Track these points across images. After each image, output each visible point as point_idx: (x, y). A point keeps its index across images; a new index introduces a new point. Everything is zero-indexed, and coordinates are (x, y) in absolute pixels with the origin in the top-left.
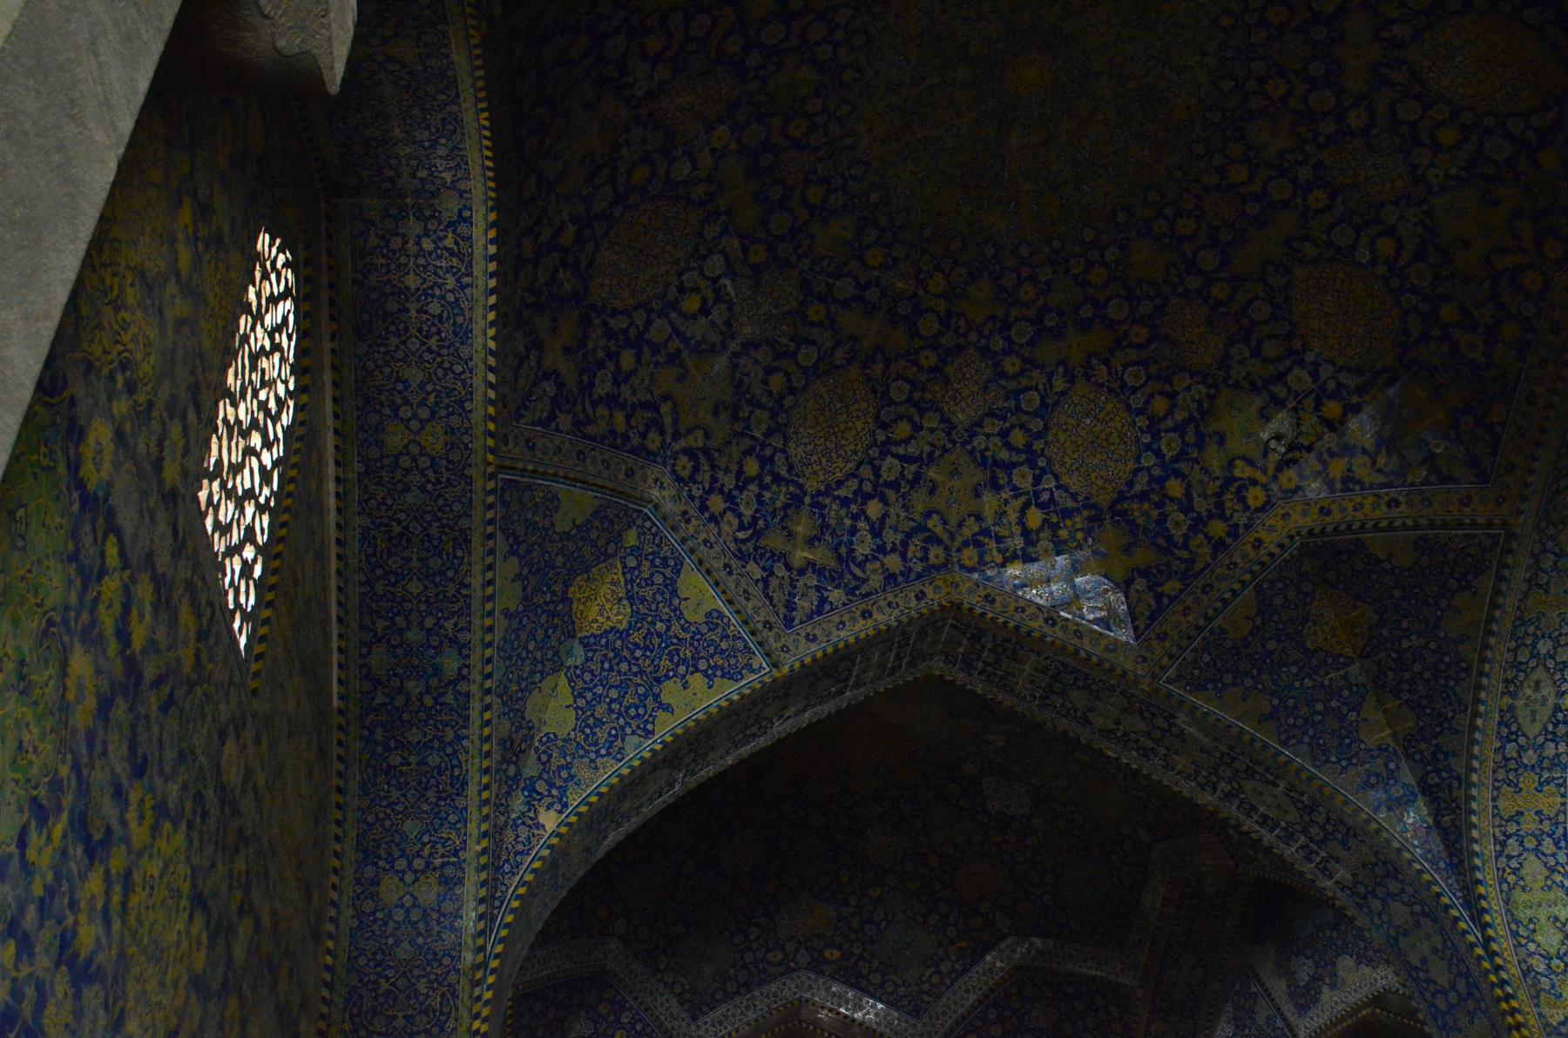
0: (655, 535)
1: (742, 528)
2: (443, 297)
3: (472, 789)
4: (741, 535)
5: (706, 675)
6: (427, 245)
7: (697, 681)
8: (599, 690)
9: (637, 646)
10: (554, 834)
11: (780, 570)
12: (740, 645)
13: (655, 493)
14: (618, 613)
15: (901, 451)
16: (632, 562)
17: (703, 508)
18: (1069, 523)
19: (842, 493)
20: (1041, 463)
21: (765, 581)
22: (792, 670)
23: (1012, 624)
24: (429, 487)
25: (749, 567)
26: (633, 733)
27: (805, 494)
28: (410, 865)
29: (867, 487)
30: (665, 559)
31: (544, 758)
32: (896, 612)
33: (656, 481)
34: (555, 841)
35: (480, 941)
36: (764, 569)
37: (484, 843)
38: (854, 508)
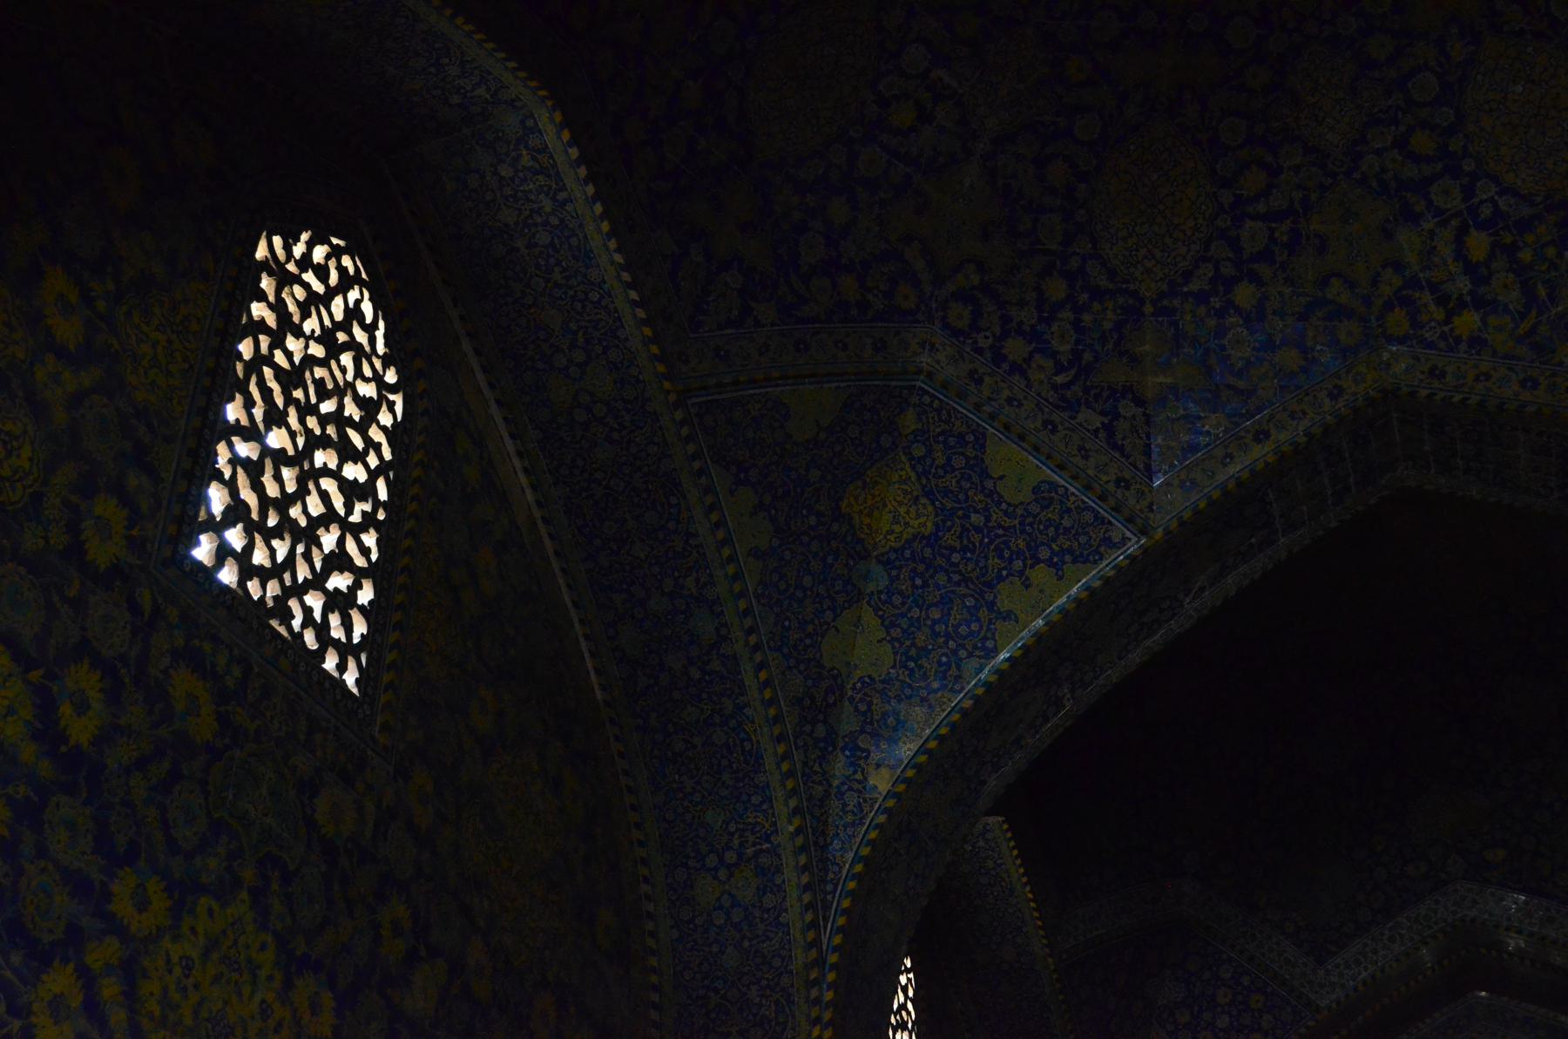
0: (939, 411)
1: (1060, 369)
2: (546, 223)
3: (769, 762)
4: (1059, 379)
5: (1050, 564)
6: (505, 171)
7: (1040, 574)
8: (916, 612)
9: (953, 549)
10: (889, 795)
11: (1127, 409)
12: (1088, 517)
13: (925, 360)
14: (918, 516)
15: (1261, 208)
16: (919, 451)
17: (998, 358)
18: (1530, 238)
19: (1194, 286)
20: (1468, 166)
21: (1109, 430)
22: (1167, 532)
23: (1474, 400)
24: (615, 435)
25: (1081, 417)
26: (970, 655)
27: (1142, 301)
28: (721, 860)
29: (1228, 270)
30: (961, 436)
31: (863, 708)
32: (1305, 423)
33: (922, 345)
34: (891, 803)
35: (811, 935)
36: (1103, 413)
37: (797, 821)
38: (1216, 302)
